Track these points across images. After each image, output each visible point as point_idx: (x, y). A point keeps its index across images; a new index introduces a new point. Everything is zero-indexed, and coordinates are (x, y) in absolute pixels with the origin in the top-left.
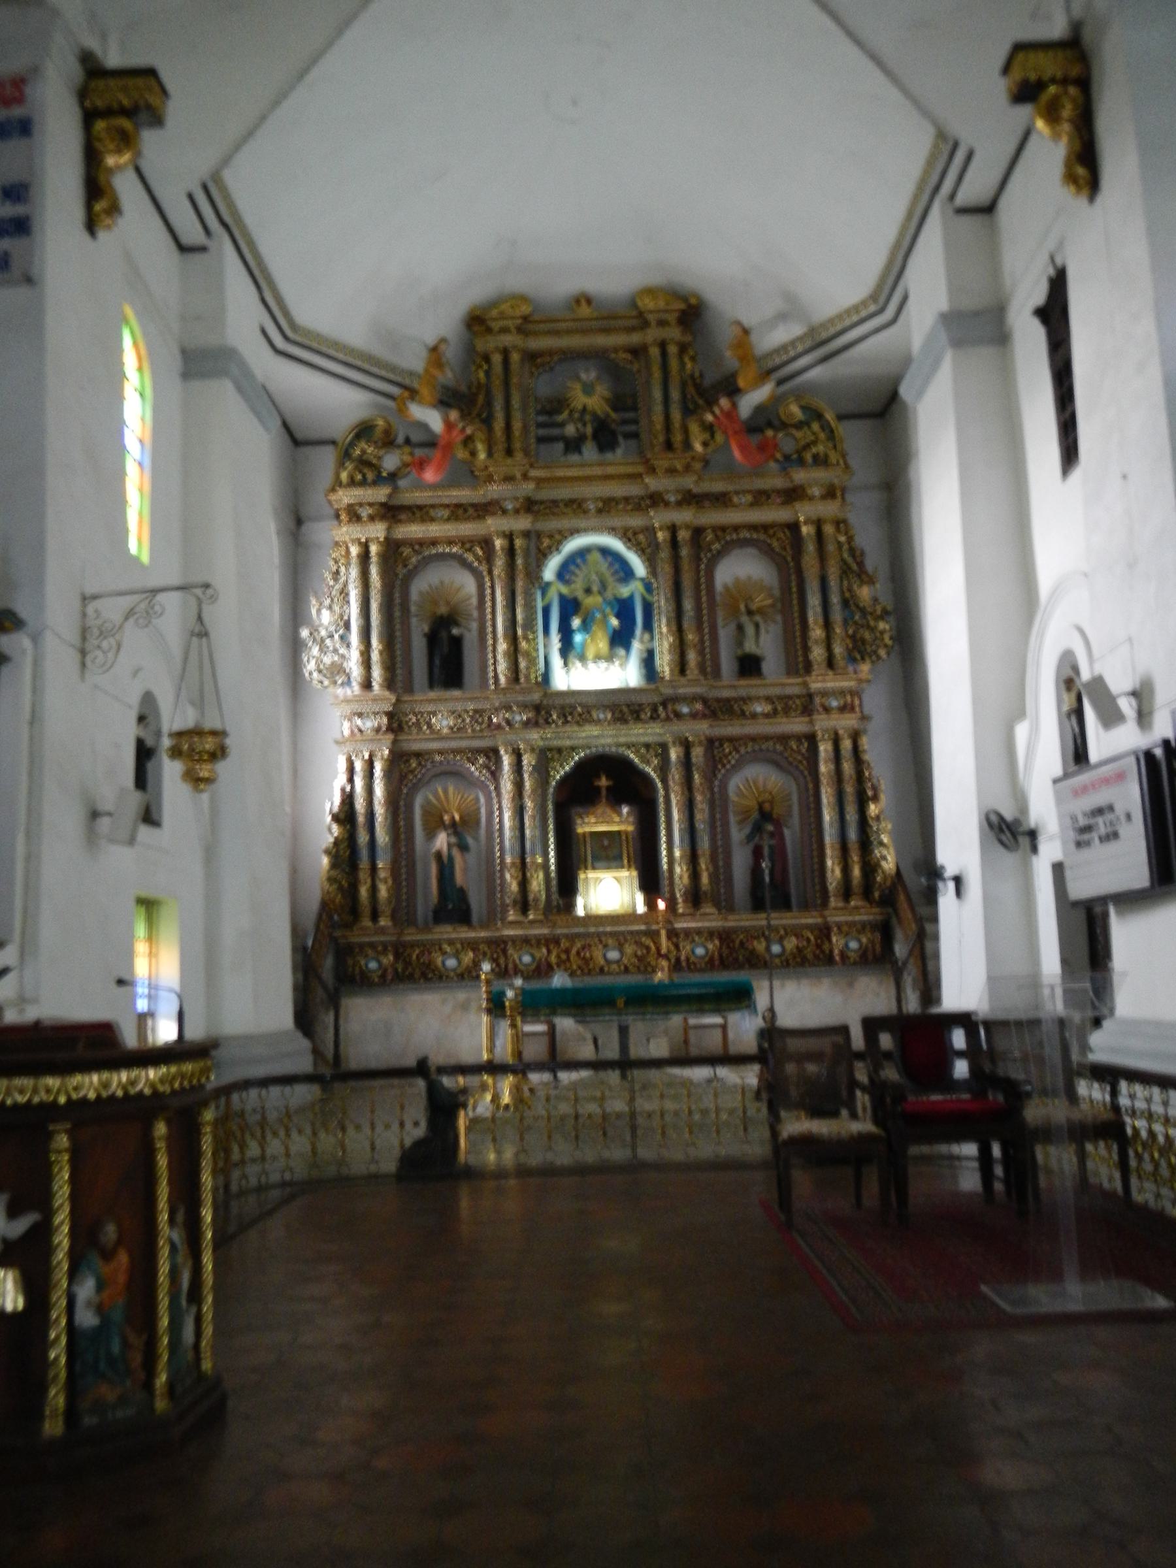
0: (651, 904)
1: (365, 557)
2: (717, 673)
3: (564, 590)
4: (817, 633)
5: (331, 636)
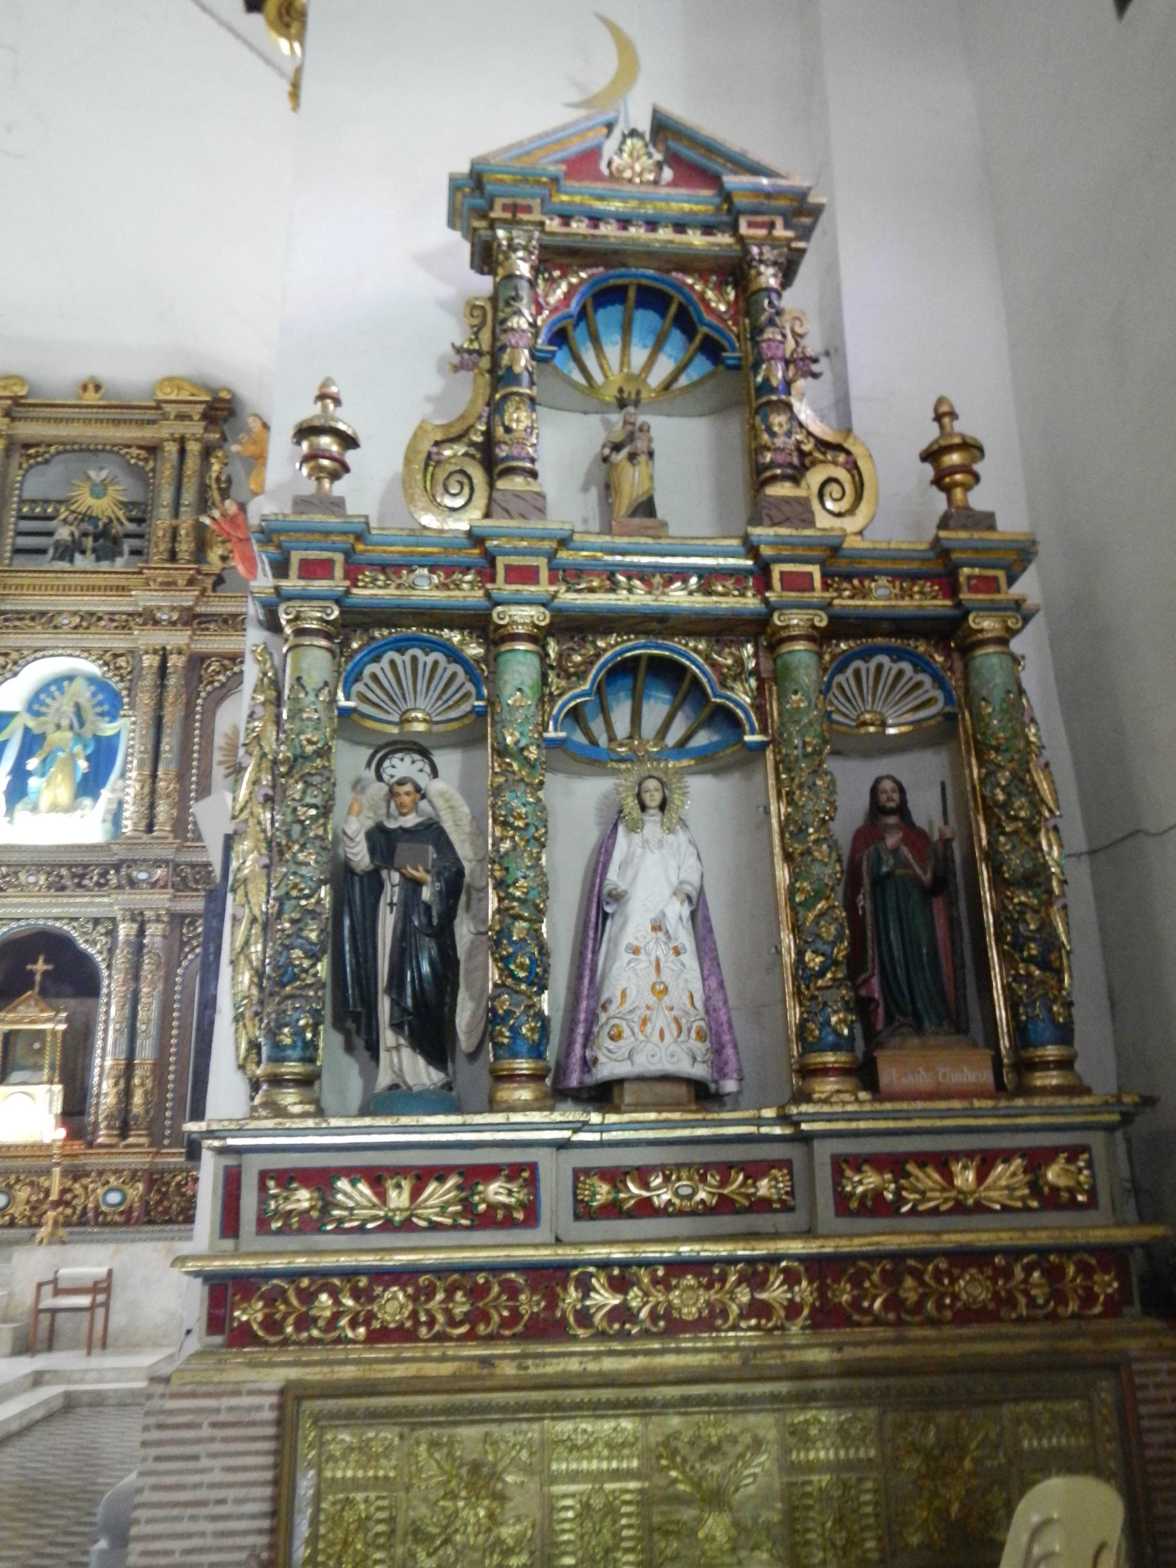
3: (31, 723)
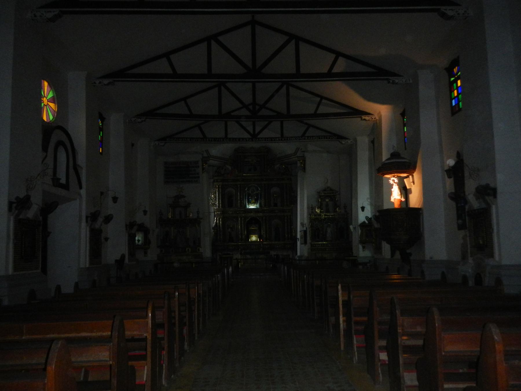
0: (260, 240)
1: (219, 188)
5: (213, 199)
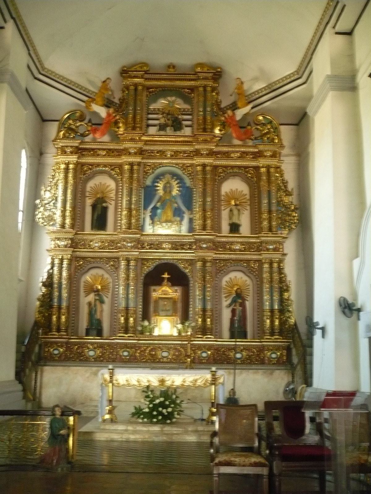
1: (67, 170)
2: (219, 231)
4: (265, 216)
